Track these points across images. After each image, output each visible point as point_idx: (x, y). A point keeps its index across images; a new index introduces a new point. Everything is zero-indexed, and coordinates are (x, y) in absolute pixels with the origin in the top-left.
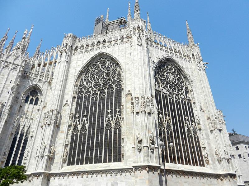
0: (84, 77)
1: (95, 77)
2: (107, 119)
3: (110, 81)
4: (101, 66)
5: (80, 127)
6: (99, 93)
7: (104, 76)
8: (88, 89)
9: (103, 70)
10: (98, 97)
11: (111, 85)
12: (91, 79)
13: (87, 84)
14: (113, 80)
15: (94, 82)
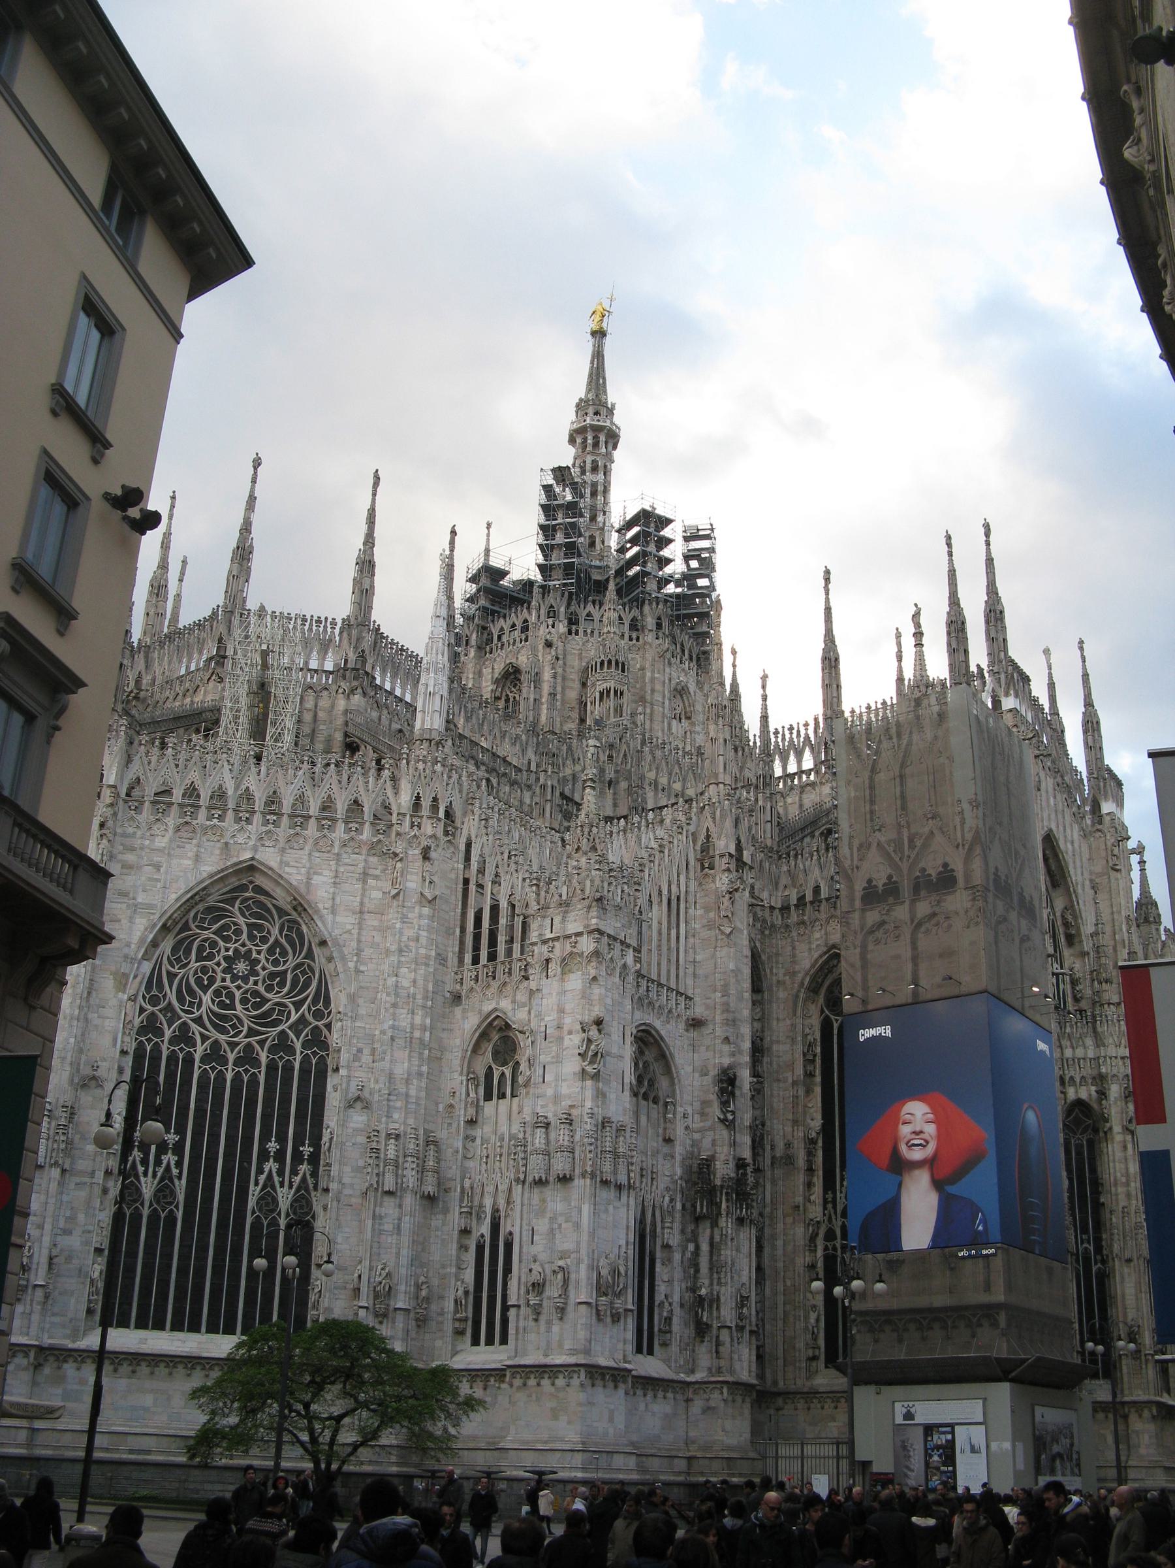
0: (165, 959)
1: (219, 979)
2: (262, 1178)
3: (281, 1013)
4: (248, 925)
5: (148, 1187)
6: (231, 1057)
7: (256, 983)
8: (184, 1023)
9: (254, 955)
10: (229, 1076)
11: (283, 1031)
12: (199, 981)
13: (181, 999)
14: (294, 1017)
15: (213, 1001)
